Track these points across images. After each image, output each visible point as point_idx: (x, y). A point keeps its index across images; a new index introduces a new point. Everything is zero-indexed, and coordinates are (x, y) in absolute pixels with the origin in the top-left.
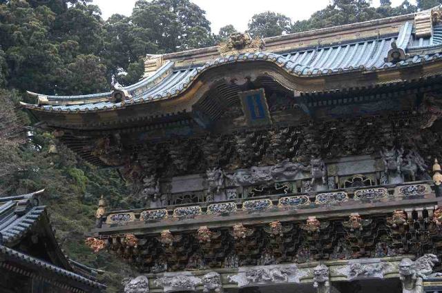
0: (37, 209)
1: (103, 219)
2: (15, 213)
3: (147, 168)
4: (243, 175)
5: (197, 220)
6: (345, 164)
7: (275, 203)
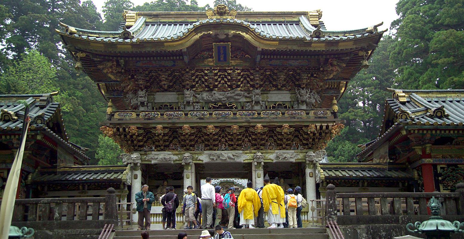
0: (52, 105)
1: (112, 115)
3: (141, 84)
4: (207, 95)
5: (181, 120)
6: (272, 95)
7: (235, 114)
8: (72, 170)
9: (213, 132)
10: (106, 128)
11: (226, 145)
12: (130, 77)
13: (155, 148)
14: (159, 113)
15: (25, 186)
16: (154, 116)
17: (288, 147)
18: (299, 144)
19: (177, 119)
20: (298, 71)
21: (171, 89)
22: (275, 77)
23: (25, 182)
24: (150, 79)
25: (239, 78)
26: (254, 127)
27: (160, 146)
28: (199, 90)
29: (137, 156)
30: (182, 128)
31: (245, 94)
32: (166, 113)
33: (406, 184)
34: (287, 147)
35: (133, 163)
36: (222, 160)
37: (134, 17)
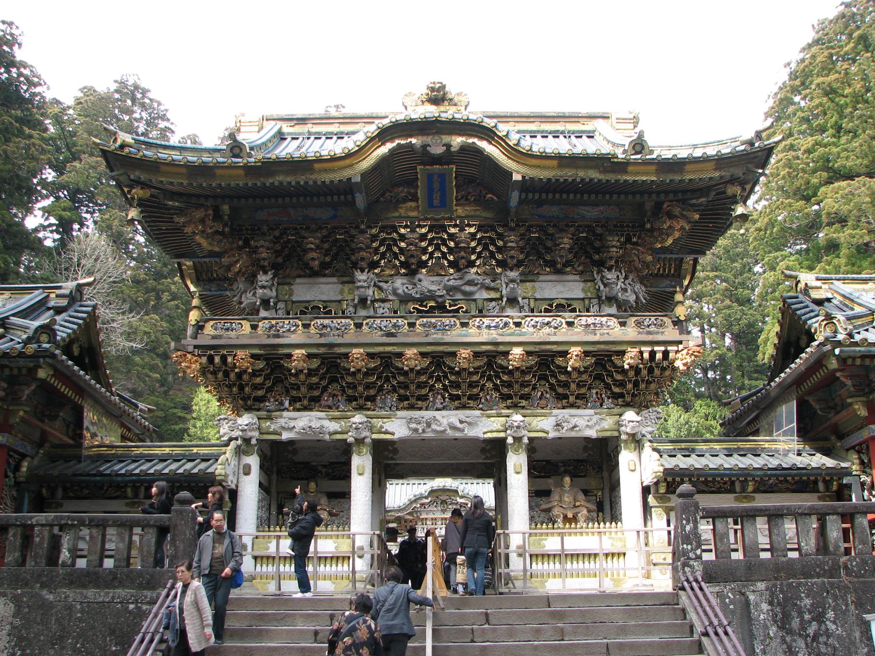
3: (264, 259)
4: (403, 284)
5: (347, 339)
6: (544, 284)
8: (113, 452)
9: (416, 366)
10: (185, 355)
11: (444, 398)
12: (240, 243)
13: (290, 403)
14: (300, 323)
15: (14, 486)
16: (289, 330)
17: (579, 402)
19: (338, 336)
20: (599, 231)
22: (549, 244)
23: (15, 477)
24: (283, 248)
25: (473, 244)
29: (251, 420)
30: (348, 358)
35: (241, 437)
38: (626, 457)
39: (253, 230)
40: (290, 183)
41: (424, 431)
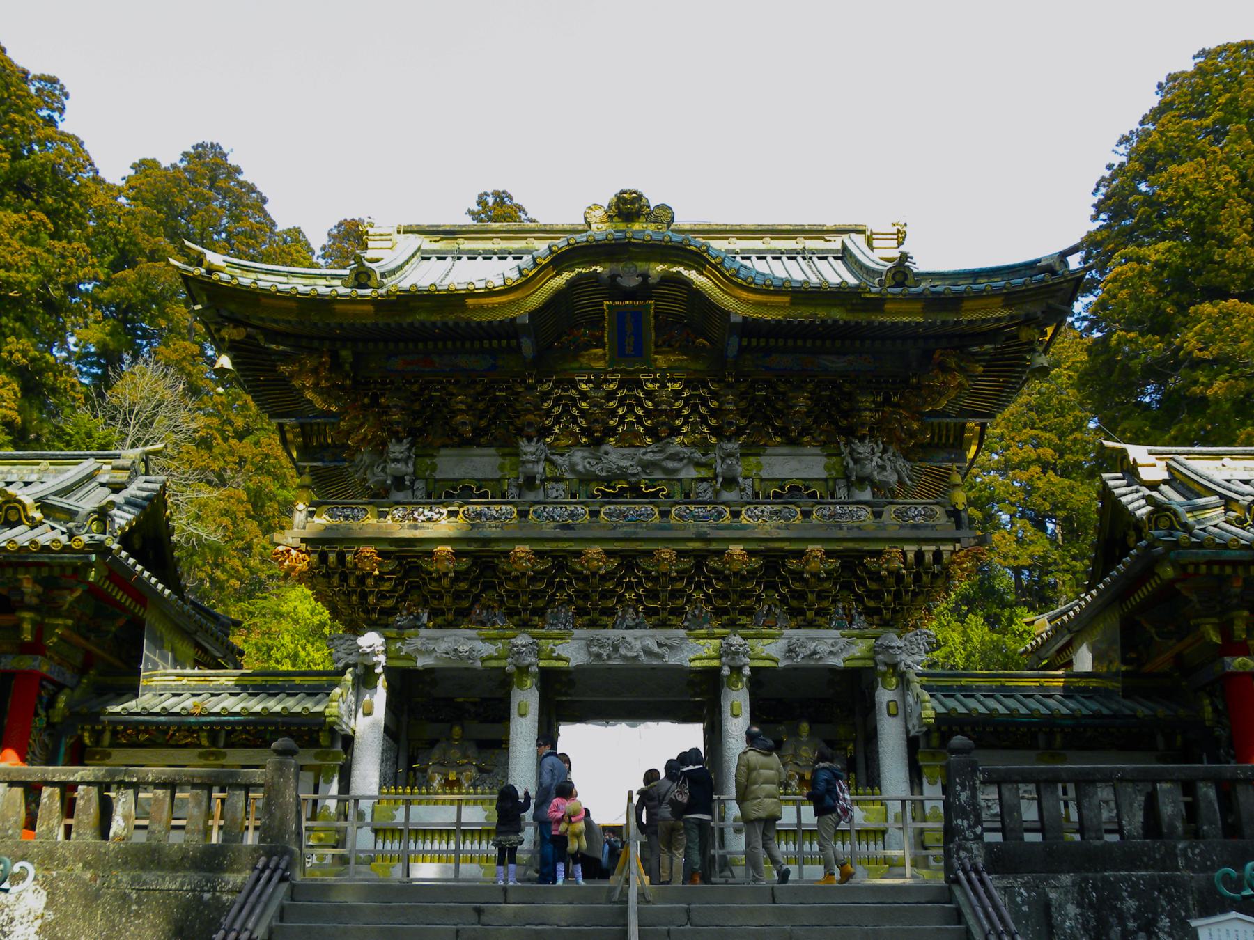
2: (102, 485)
3: (398, 423)
4: (585, 458)
5: (508, 533)
7: (665, 514)
10: (288, 551)
11: (637, 612)
12: (366, 401)
15: (46, 729)
17: (820, 620)
18: (853, 612)
19: (496, 527)
20: (847, 388)
21: (482, 440)
22: (780, 405)
23: (48, 716)
25: (678, 405)
26: (720, 553)
27: (443, 613)
28: (563, 442)
31: (696, 455)
32: (465, 508)
33: (1179, 738)
34: (818, 618)
36: (625, 657)
37: (390, 235)
38: (885, 696)
39: (384, 383)
40: (434, 324)
41: (609, 657)
